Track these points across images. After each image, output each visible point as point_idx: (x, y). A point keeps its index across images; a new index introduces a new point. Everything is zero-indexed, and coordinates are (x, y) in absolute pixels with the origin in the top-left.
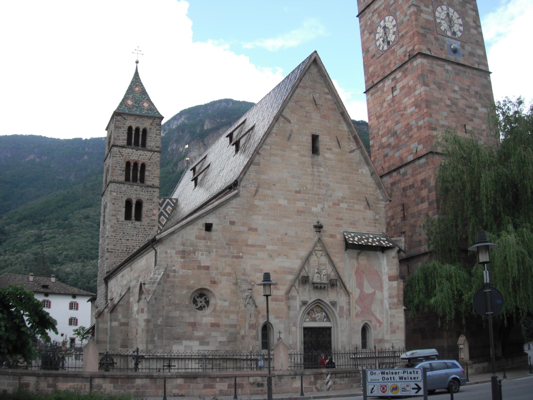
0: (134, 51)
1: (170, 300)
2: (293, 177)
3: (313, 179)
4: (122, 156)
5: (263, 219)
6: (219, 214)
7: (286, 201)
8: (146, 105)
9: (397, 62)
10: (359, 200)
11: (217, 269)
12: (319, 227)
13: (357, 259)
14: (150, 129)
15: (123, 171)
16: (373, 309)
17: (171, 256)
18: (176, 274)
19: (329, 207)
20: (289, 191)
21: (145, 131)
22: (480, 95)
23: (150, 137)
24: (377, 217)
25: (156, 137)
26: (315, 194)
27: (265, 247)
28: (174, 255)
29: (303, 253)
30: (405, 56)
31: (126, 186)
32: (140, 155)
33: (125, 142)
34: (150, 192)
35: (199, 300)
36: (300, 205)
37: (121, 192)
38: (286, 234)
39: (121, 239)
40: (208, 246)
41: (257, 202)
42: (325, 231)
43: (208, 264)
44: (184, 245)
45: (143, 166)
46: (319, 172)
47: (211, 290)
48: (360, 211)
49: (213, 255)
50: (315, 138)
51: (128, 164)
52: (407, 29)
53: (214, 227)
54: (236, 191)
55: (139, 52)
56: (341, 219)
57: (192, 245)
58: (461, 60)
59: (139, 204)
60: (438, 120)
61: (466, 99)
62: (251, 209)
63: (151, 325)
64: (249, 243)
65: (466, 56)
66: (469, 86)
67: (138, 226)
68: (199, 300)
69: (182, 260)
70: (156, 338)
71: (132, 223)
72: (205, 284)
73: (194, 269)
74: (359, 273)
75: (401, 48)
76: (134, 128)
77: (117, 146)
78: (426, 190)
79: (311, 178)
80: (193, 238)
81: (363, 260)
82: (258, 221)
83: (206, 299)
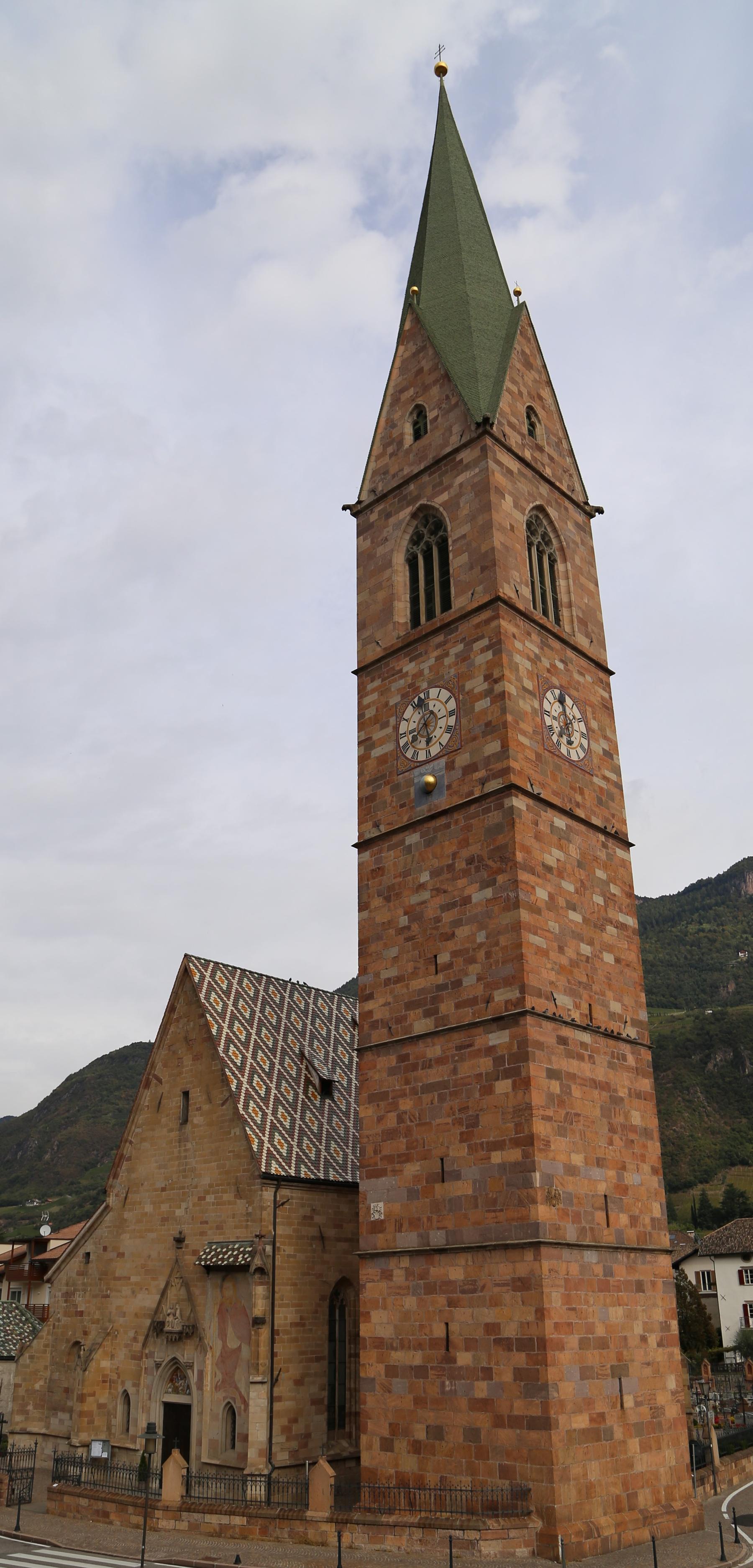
2: (160, 1167)
3: (179, 1165)
5: (130, 1238)
10: (228, 1184)
11: (89, 1314)
12: (179, 1241)
13: (222, 1287)
16: (236, 1377)
19: (194, 1205)
20: (156, 1190)
22: (481, 859)
24: (250, 1209)
27: (129, 1278)
29: (162, 1286)
36: (165, 1207)
38: (149, 1256)
40: (84, 1284)
42: (187, 1246)
44: (67, 1285)
46: (186, 1150)
48: (229, 1203)
49: (88, 1294)
50: (186, 1094)
56: (206, 1222)
58: (442, 801)
60: (377, 975)
61: (445, 892)
62: (121, 1225)
63: (21, 1392)
64: (117, 1275)
65: (454, 785)
66: (454, 855)
70: (30, 1407)
74: (222, 1313)
79: (177, 1163)
80: (74, 1275)
81: (229, 1288)
82: (128, 1243)
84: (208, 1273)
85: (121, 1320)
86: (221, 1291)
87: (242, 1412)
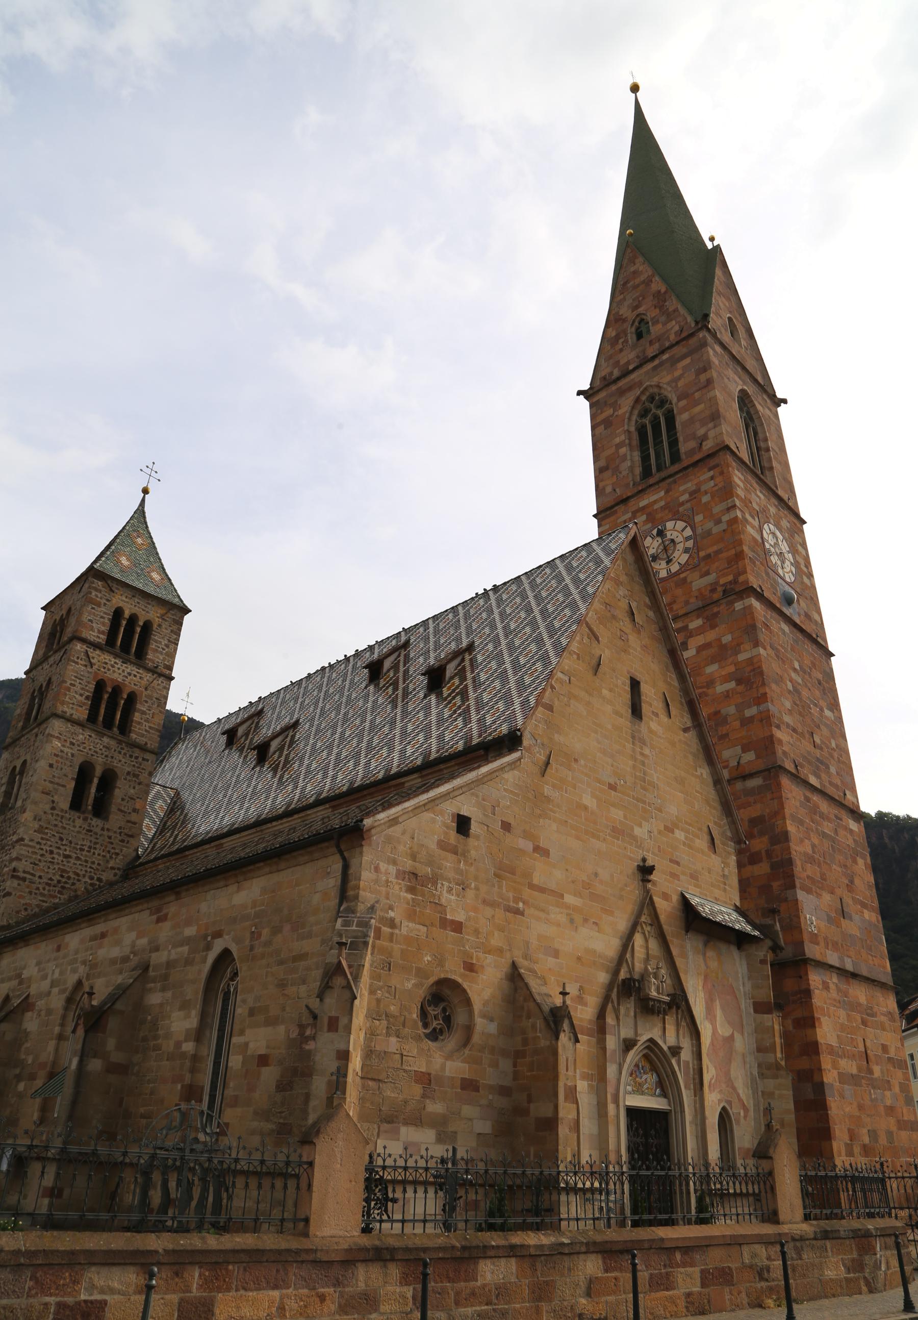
0: (145, 469)
1: (378, 1001)
4: (92, 665)
6: (483, 800)
7: (595, 801)
8: (155, 576)
9: (693, 600)
11: (477, 932)
13: (704, 955)
14: (160, 626)
15: (87, 698)
17: (387, 881)
18: (397, 931)
20: (599, 781)
21: (147, 627)
23: (156, 641)
25: (167, 646)
26: (638, 800)
28: (392, 879)
30: (713, 590)
31: (87, 733)
32: (130, 674)
33: (103, 637)
34: (137, 758)
35: (432, 1011)
36: (617, 814)
37: (73, 744)
38: (596, 875)
39: (51, 852)
41: (547, 790)
43: (460, 917)
44: (414, 857)
45: (132, 699)
47: (465, 985)
49: (470, 893)
51: (100, 685)
52: (721, 546)
53: (474, 828)
54: (515, 755)
55: (153, 474)
57: (430, 863)
59: (108, 780)
67: (98, 830)
68: (432, 1011)
69: (409, 896)
71: (85, 819)
72: (454, 971)
73: (432, 924)
75: (701, 577)
76: (127, 614)
77: (84, 641)
78: (765, 839)
82: (550, 833)
83: (444, 1010)
84: (687, 931)
85: (551, 961)
86: (705, 961)
87: (742, 1120)
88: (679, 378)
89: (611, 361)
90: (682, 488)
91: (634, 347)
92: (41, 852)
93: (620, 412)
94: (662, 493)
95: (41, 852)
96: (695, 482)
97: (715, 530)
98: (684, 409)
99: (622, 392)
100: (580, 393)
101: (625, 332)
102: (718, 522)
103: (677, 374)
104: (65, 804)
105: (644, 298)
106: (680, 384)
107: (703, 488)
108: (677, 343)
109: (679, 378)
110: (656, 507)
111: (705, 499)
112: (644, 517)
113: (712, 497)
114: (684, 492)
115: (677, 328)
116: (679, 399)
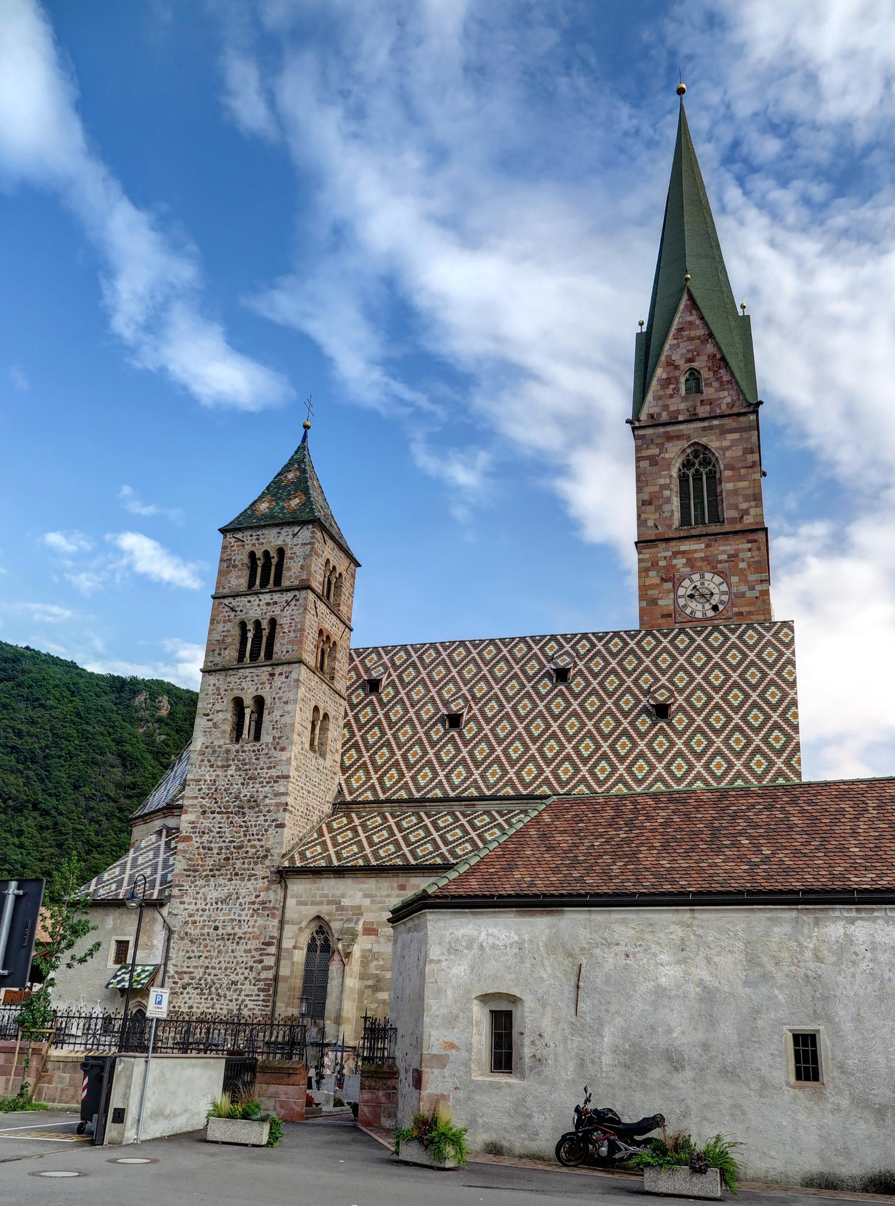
67: (321, 768)
77: (313, 591)
88: (728, 448)
89: (660, 403)
90: (721, 548)
91: (685, 399)
92: (298, 788)
93: (667, 456)
94: (703, 546)
95: (298, 788)
96: (736, 547)
97: (749, 594)
98: (729, 480)
99: (670, 438)
100: (628, 421)
101: (677, 379)
102: (752, 588)
103: (726, 443)
104: (307, 746)
105: (698, 355)
106: (728, 454)
107: (741, 555)
108: (730, 415)
109: (728, 448)
110: (696, 555)
111: (742, 565)
112: (684, 561)
113: (749, 566)
114: (724, 552)
115: (729, 400)
116: (727, 467)
